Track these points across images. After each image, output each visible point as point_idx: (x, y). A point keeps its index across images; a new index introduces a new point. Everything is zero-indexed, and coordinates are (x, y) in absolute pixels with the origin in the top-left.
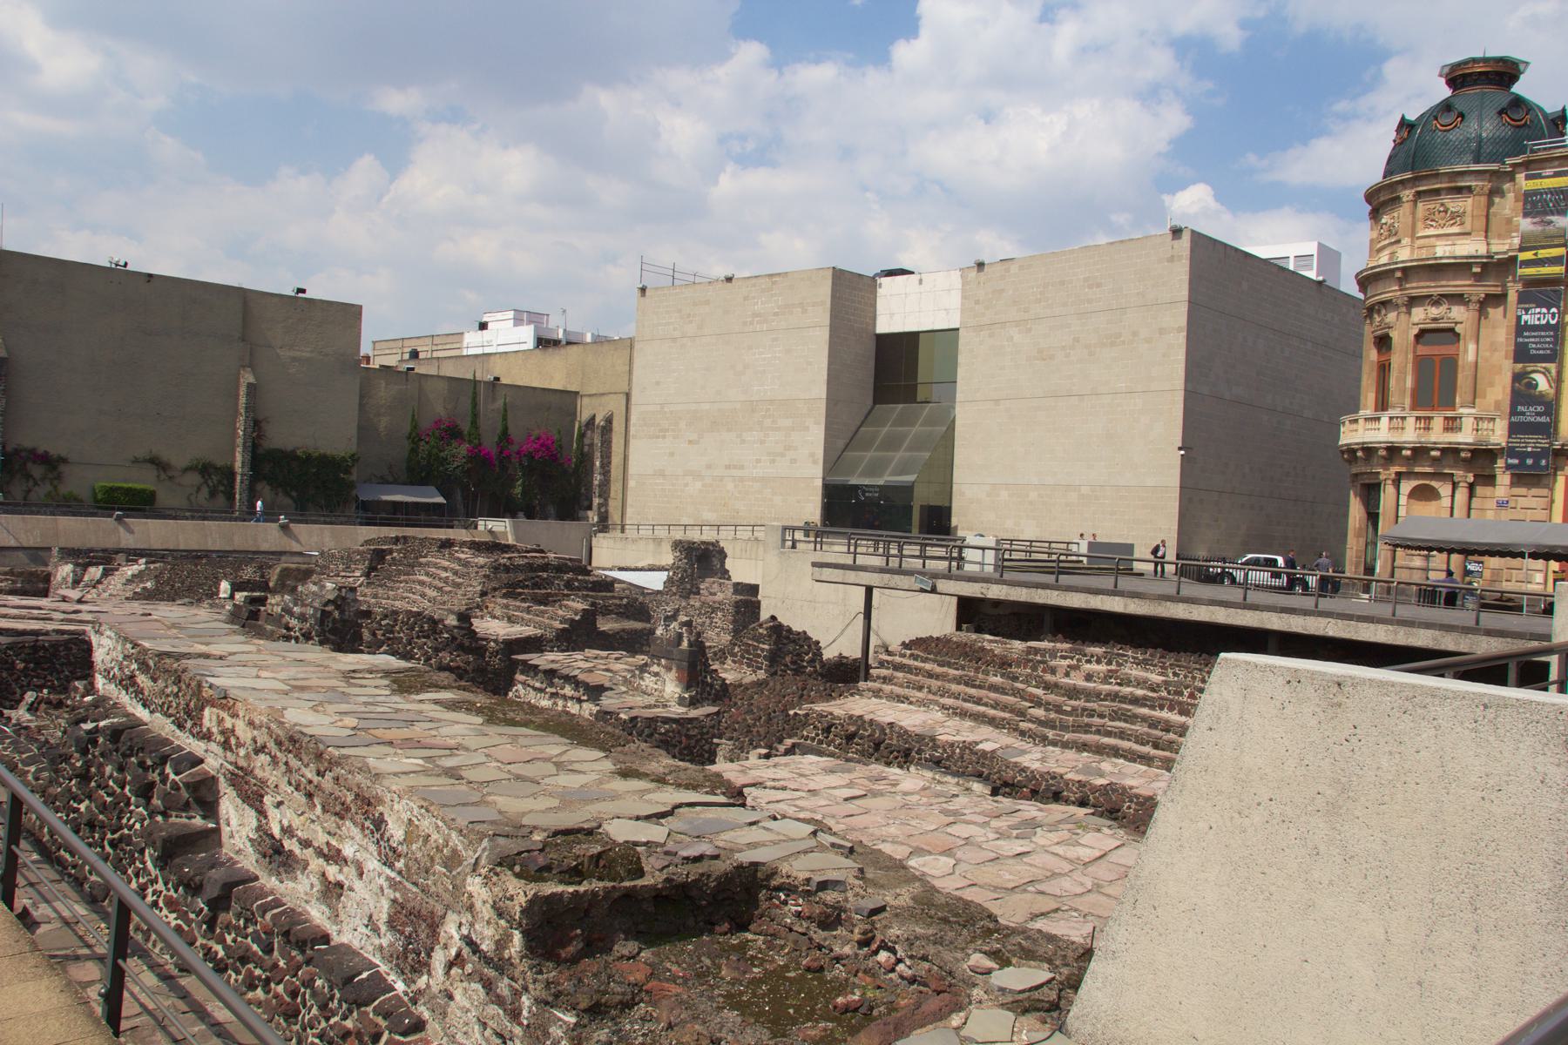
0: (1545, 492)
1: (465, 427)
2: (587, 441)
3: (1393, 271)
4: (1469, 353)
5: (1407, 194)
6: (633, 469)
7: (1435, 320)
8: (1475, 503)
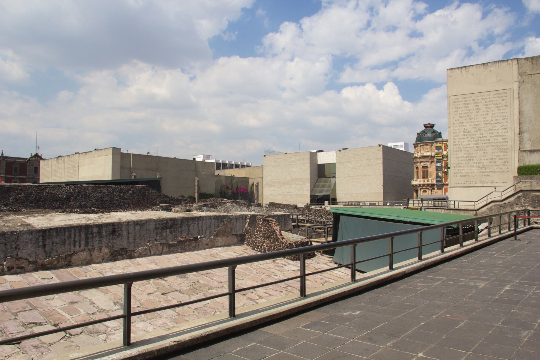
0: (441, 190)
1: (230, 187)
2: (252, 188)
3: (418, 157)
4: (430, 170)
5: (419, 145)
6: (264, 194)
7: (425, 165)
8: (432, 192)
